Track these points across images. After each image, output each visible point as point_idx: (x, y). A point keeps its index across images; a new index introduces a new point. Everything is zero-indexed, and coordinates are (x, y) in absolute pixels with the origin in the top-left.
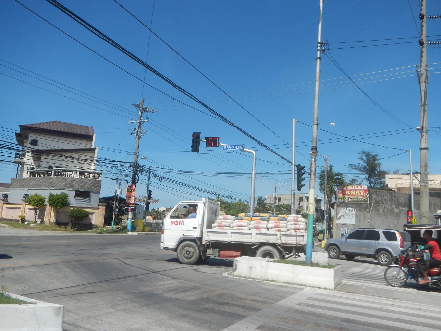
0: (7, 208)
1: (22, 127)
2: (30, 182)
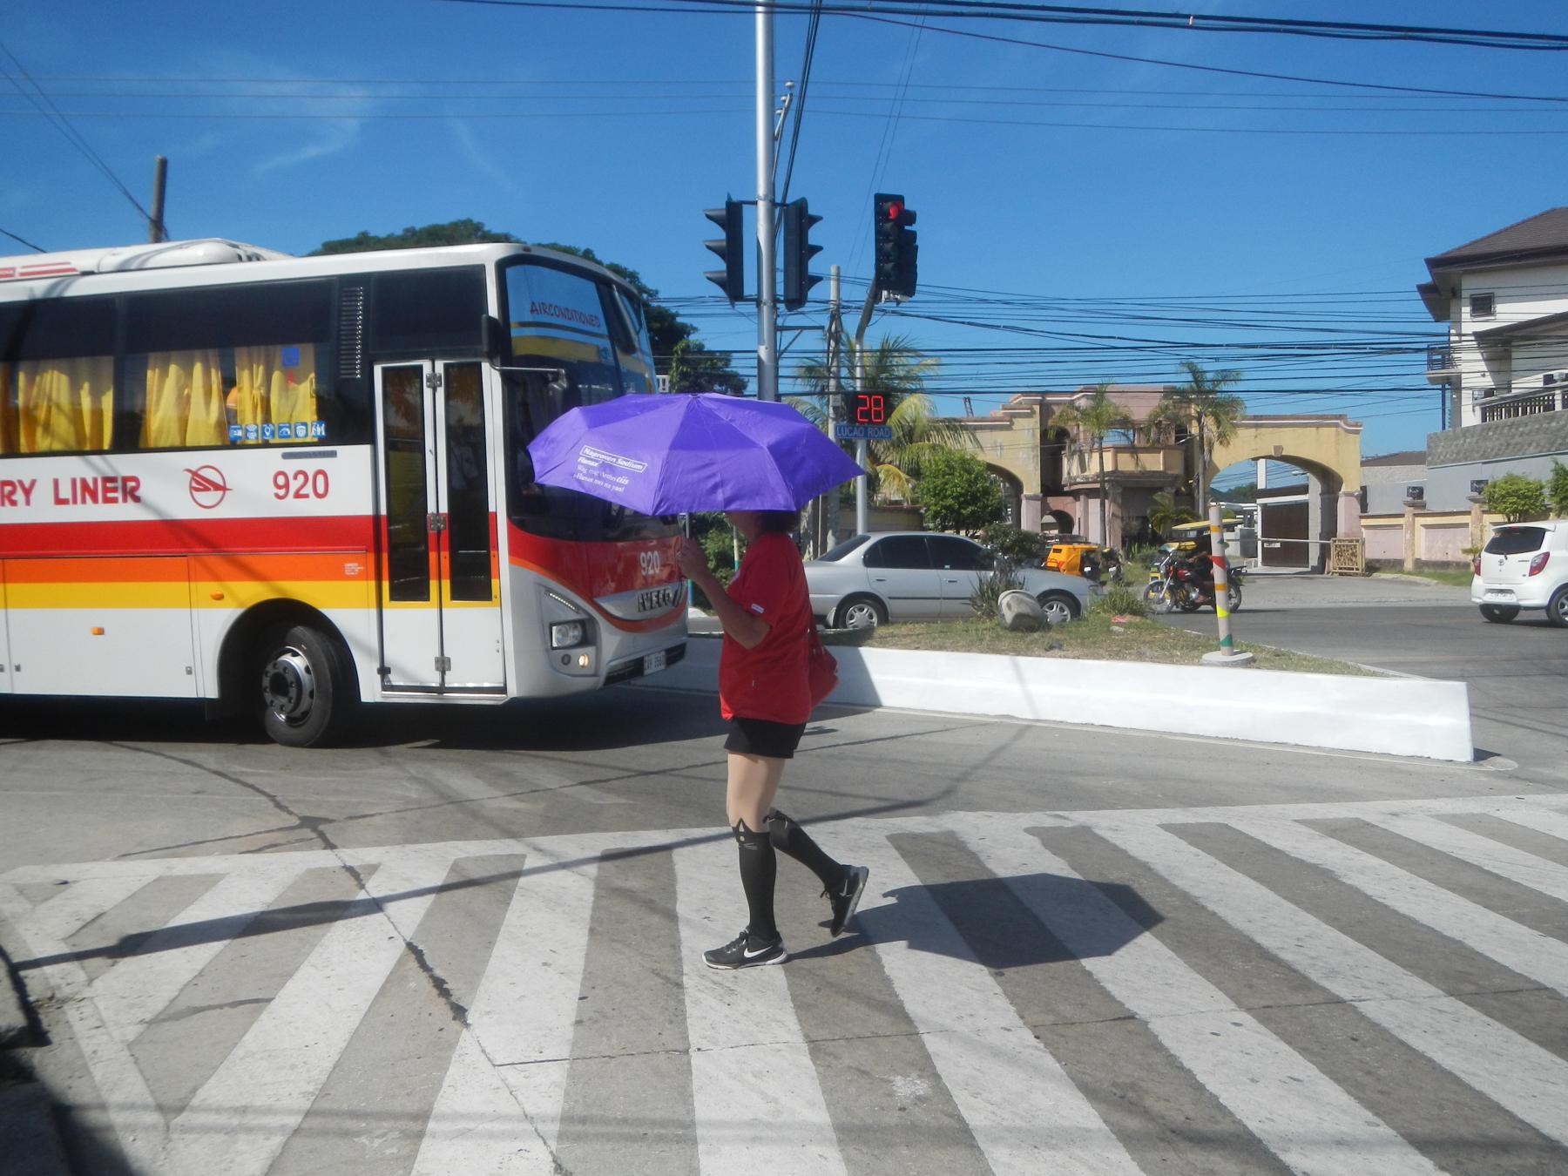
0: (1427, 527)
1: (1433, 263)
2: (1485, 439)
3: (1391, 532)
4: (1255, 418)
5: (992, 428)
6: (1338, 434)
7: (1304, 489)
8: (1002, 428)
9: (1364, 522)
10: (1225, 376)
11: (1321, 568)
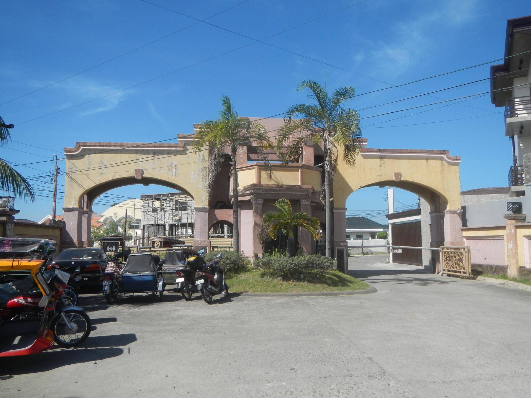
3: (491, 242)
4: (380, 151)
5: (169, 153)
6: (443, 165)
7: (417, 212)
8: (177, 153)
9: (465, 234)
10: (343, 94)
11: (432, 269)
